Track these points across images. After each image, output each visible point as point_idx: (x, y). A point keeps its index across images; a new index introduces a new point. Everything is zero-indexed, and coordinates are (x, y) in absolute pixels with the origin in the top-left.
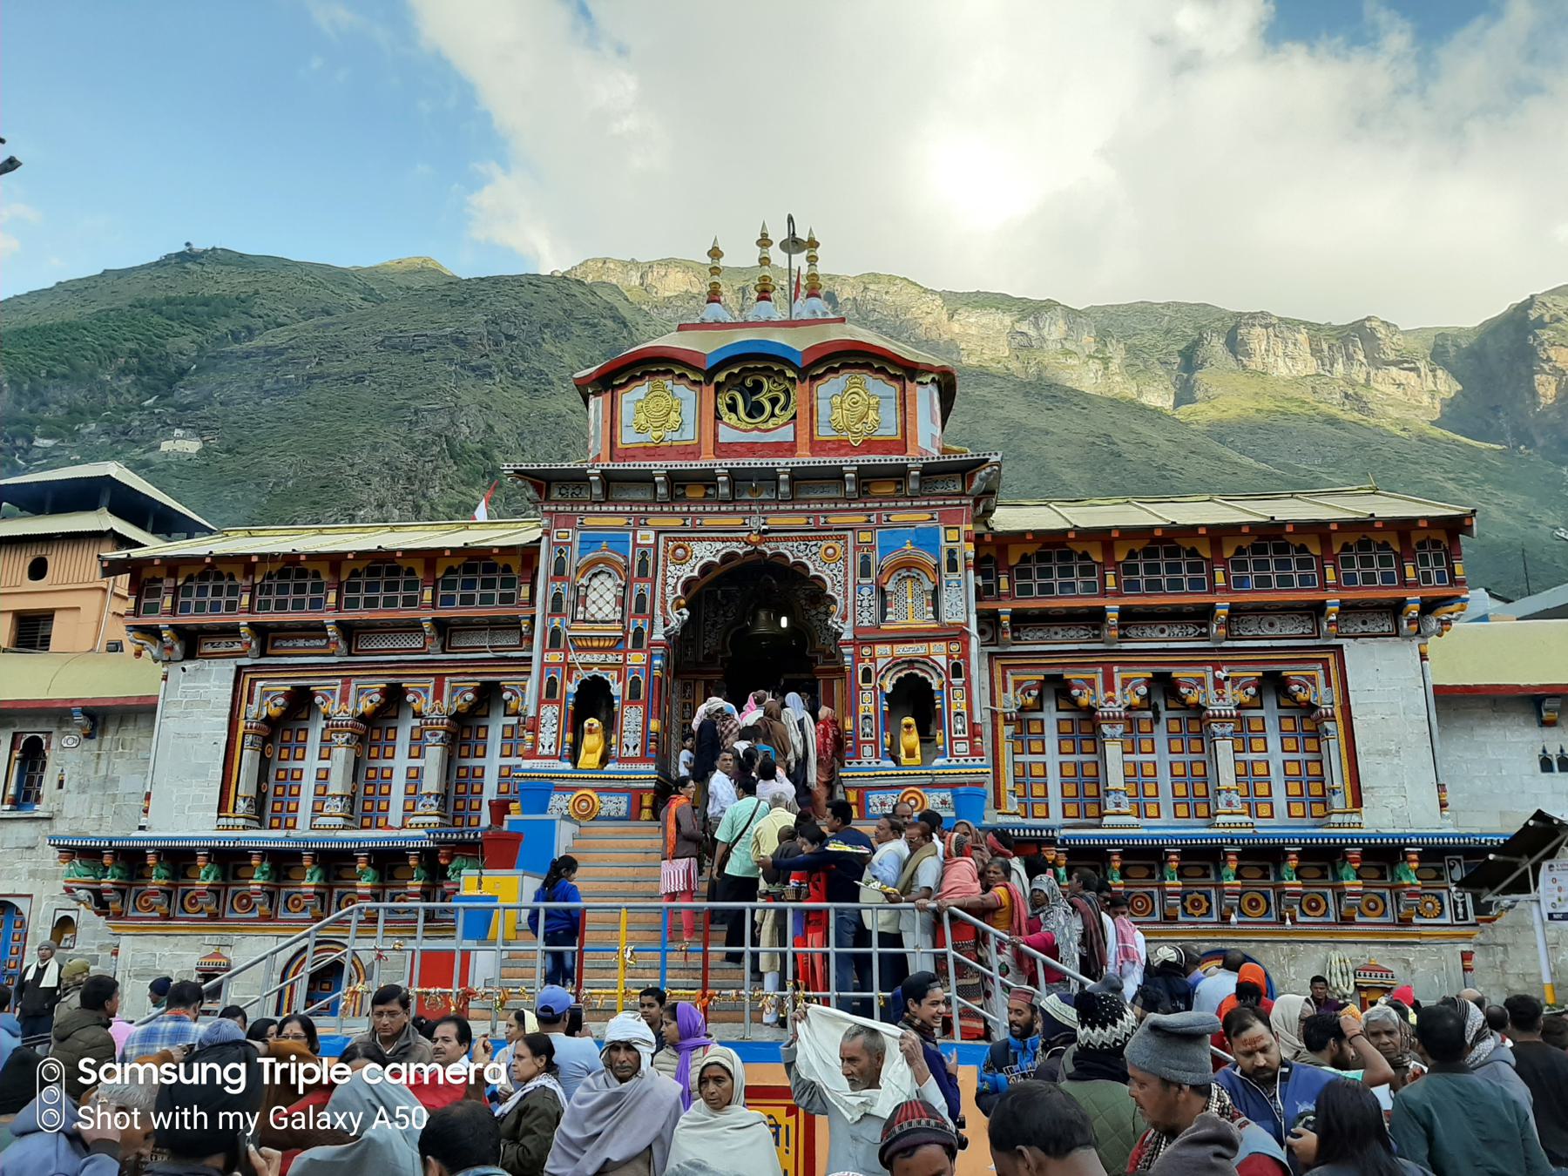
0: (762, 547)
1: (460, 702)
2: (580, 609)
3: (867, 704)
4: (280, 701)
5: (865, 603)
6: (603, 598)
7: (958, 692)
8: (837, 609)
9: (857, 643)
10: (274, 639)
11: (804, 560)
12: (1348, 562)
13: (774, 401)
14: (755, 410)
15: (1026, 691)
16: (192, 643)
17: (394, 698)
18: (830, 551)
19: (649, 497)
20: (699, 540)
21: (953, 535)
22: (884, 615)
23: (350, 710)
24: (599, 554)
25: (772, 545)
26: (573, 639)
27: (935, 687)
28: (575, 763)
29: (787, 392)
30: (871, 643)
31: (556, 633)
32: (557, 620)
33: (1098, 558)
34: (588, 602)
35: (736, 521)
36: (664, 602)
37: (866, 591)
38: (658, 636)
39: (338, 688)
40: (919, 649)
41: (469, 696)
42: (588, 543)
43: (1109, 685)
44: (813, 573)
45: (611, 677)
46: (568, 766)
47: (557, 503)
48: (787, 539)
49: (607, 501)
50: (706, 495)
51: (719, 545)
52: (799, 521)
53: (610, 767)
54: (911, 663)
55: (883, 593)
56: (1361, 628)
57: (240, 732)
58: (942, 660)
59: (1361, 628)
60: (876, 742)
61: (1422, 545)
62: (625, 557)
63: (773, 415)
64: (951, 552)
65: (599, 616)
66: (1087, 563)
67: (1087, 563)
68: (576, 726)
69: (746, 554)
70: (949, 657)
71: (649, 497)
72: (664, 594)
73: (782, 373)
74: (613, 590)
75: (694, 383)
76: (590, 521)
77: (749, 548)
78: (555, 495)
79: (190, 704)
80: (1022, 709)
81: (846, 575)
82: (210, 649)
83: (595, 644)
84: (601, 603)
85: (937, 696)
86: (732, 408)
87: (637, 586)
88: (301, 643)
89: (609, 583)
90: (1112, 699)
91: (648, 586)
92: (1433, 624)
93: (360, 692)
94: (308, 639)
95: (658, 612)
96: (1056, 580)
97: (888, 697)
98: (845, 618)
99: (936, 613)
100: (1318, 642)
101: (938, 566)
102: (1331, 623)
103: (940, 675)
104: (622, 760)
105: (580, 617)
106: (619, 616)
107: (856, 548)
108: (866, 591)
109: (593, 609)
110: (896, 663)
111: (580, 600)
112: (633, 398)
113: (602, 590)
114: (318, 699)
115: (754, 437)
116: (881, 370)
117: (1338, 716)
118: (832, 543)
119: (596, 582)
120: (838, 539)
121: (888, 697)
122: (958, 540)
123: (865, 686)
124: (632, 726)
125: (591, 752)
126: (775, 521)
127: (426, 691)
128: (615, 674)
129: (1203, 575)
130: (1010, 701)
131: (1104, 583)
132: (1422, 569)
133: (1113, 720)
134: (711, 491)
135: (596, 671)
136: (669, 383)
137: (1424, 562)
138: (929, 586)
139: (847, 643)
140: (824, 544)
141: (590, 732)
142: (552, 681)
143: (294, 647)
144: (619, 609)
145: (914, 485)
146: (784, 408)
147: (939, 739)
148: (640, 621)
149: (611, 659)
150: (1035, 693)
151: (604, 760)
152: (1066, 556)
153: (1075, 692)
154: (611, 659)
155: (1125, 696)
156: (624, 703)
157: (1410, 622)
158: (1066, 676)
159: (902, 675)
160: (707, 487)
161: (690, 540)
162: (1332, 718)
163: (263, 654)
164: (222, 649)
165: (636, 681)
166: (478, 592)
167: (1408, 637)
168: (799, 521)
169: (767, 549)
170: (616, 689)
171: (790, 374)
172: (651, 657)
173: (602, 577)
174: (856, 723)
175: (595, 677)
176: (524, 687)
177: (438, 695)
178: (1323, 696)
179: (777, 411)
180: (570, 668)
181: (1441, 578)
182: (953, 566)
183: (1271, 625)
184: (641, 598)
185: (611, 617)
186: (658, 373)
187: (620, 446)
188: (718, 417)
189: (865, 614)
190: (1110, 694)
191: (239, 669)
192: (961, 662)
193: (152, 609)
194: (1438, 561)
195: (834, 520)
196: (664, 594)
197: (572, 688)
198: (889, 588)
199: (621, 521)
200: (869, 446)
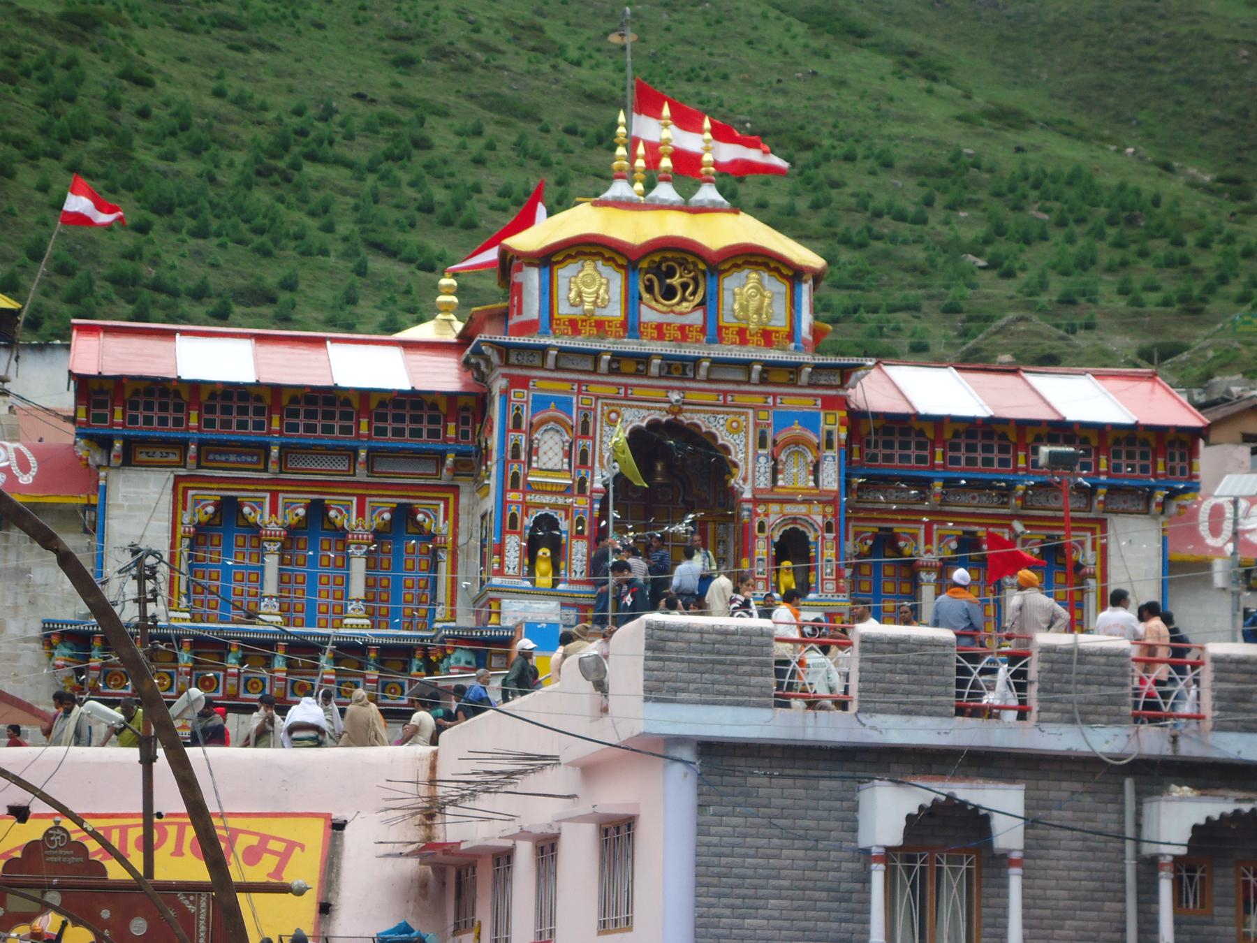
0: (681, 417)
1: (379, 520)
2: (534, 458)
3: (762, 549)
4: (210, 509)
5: (762, 470)
6: (551, 449)
7: (829, 544)
8: (740, 473)
9: (756, 501)
10: (207, 455)
11: (713, 430)
12: (1117, 455)
13: (685, 286)
14: (669, 293)
15: (863, 541)
16: (134, 454)
17: (317, 510)
18: (735, 425)
19: (591, 368)
20: (631, 407)
21: (831, 419)
22: (774, 480)
23: (280, 522)
24: (551, 413)
25: (688, 415)
26: (529, 484)
27: (811, 539)
28: (533, 582)
29: (695, 279)
30: (766, 502)
31: (516, 476)
32: (516, 467)
33: (930, 435)
34: (541, 452)
35: (659, 394)
36: (602, 457)
37: (762, 460)
38: (598, 485)
39: (268, 500)
40: (802, 509)
41: (387, 516)
42: (540, 403)
43: (928, 540)
44: (720, 442)
45: (560, 516)
46: (527, 584)
47: (514, 366)
48: (698, 412)
49: (557, 369)
50: (638, 370)
51: (645, 413)
52: (710, 398)
53: (561, 586)
54: (794, 520)
55: (775, 459)
56: (1122, 506)
57: (179, 536)
58: (819, 519)
59: (1122, 506)
60: (767, 580)
61: (1172, 444)
62: (571, 418)
63: (683, 299)
64: (829, 433)
65: (550, 466)
66: (922, 439)
67: (922, 439)
68: (531, 553)
69: (667, 422)
70: (824, 516)
71: (591, 368)
72: (601, 450)
73: (695, 265)
74: (560, 444)
75: (620, 266)
76: (540, 384)
77: (670, 417)
78: (513, 359)
79: (130, 508)
80: (859, 556)
81: (746, 445)
82: (143, 457)
83: (549, 489)
84: (550, 454)
85: (812, 547)
86: (649, 289)
87: (580, 442)
88: (232, 458)
89: (557, 438)
90: (928, 551)
91: (589, 442)
92: (1173, 508)
93: (287, 506)
94: (239, 454)
95: (597, 465)
96: (897, 452)
97: (776, 545)
98: (745, 480)
99: (816, 481)
100: (1091, 515)
101: (818, 447)
102: (1100, 502)
103: (816, 530)
104: (572, 582)
105: (534, 465)
106: (566, 467)
107: (756, 425)
108: (762, 460)
109: (544, 458)
110: (784, 523)
111: (532, 451)
112: (564, 274)
113: (551, 443)
114: (246, 510)
115: (670, 318)
116: (777, 270)
117: (1098, 574)
118: (736, 418)
119: (547, 437)
120: (741, 414)
121: (776, 545)
122: (834, 424)
123: (760, 535)
124: (579, 556)
125: (544, 575)
126: (692, 397)
127: (348, 509)
128: (563, 514)
129: (1009, 456)
130: (850, 547)
131: (933, 458)
132: (1170, 464)
133: (929, 568)
134: (641, 367)
135: (547, 510)
136: (600, 263)
137: (1172, 459)
138: (810, 457)
139: (747, 501)
140: (731, 418)
141: (542, 559)
142: (514, 516)
143: (227, 461)
144: (566, 460)
145: (804, 378)
146: (694, 293)
147: (812, 578)
148: (583, 472)
149: (561, 500)
150: (870, 542)
151: (555, 583)
152: (906, 431)
153: (902, 544)
154: (561, 500)
155: (940, 549)
156: (573, 537)
157: (1158, 505)
158: (896, 530)
159: (788, 528)
160: (638, 363)
161: (622, 406)
162: (1093, 576)
163: (199, 467)
164: (157, 458)
165: (580, 521)
166: (407, 426)
167: (1155, 517)
168: (710, 398)
169: (685, 418)
170: (564, 525)
171: (702, 266)
172: (592, 501)
173: (551, 433)
174: (752, 564)
175: (546, 515)
176: (436, 511)
177: (361, 513)
178: (1089, 557)
179: (687, 293)
180: (527, 507)
181: (1183, 473)
182: (829, 445)
183: (1056, 498)
184: (584, 454)
185: (559, 467)
186: (591, 254)
187: (556, 316)
188: (641, 298)
189: (762, 478)
190: (929, 547)
191: (178, 479)
192: (833, 521)
193: (102, 418)
194: (1182, 459)
195: (740, 399)
196: (601, 450)
197: (529, 522)
198: (783, 457)
199: (566, 386)
200: (767, 337)
